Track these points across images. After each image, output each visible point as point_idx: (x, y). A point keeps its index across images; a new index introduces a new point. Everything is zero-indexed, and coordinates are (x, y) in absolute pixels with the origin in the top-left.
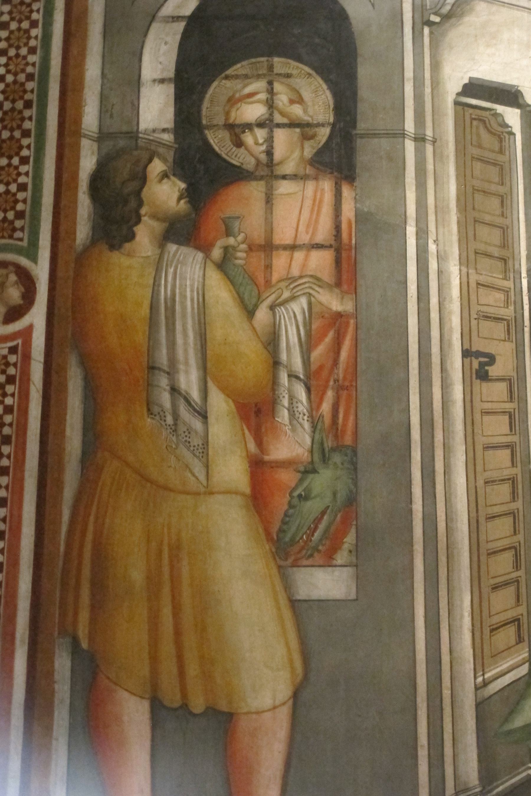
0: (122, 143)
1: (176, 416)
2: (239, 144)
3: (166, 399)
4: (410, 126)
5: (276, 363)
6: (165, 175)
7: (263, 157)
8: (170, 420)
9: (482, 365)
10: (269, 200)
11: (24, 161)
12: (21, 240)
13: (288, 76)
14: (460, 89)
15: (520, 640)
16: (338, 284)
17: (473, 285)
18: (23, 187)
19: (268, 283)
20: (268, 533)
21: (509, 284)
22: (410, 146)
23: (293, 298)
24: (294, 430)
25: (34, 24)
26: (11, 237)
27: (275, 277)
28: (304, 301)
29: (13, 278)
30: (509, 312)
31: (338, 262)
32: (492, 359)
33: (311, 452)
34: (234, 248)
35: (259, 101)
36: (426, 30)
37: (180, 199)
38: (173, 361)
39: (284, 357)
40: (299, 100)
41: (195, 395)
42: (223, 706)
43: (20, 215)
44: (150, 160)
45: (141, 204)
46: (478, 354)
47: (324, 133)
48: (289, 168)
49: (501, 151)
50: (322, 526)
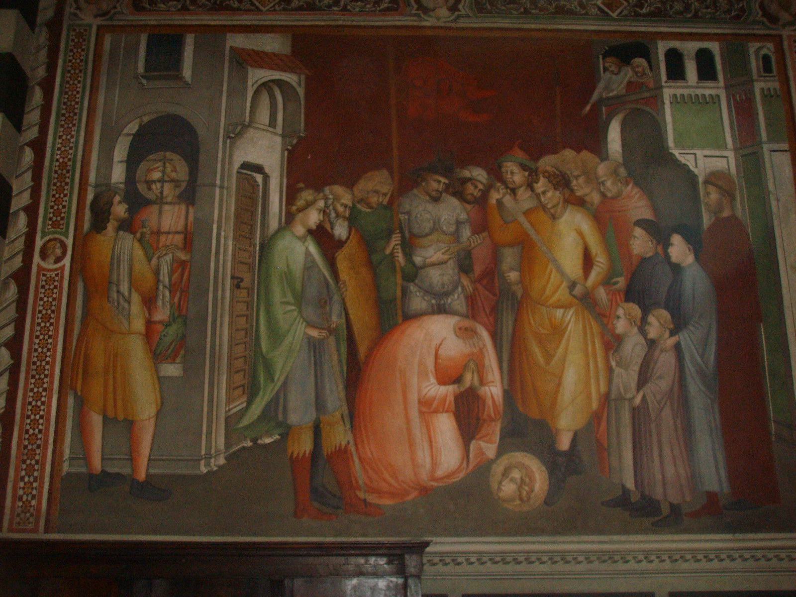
0: (104, 188)
1: (118, 303)
2: (150, 189)
3: (115, 295)
4: (218, 182)
5: (158, 281)
6: (120, 202)
7: (159, 195)
8: (116, 304)
9: (239, 283)
10: (160, 213)
11: (65, 195)
12: (62, 229)
13: (172, 160)
14: (239, 166)
15: (244, 393)
16: (185, 248)
17: (237, 250)
18: (64, 207)
19: (157, 248)
20: (151, 351)
21: (252, 249)
22: (217, 190)
23: (167, 254)
24: (163, 308)
25: (72, 137)
26: (58, 228)
27: (161, 245)
28: (171, 255)
29: (58, 245)
30: (250, 261)
31: (185, 238)
32: (242, 280)
33: (169, 317)
34: (146, 233)
35: (159, 171)
36: (228, 141)
37: (125, 212)
38: (118, 280)
39: (161, 278)
40: (174, 170)
41: (126, 294)
42: (130, 418)
43: (62, 218)
44: (115, 196)
45: (110, 215)
46: (238, 278)
47: (184, 185)
48: (169, 199)
49: (253, 193)
50: (171, 348)
